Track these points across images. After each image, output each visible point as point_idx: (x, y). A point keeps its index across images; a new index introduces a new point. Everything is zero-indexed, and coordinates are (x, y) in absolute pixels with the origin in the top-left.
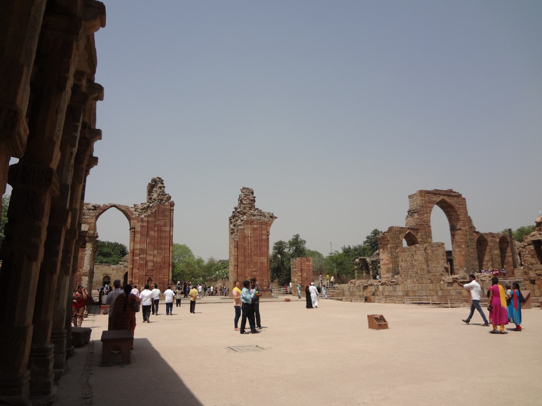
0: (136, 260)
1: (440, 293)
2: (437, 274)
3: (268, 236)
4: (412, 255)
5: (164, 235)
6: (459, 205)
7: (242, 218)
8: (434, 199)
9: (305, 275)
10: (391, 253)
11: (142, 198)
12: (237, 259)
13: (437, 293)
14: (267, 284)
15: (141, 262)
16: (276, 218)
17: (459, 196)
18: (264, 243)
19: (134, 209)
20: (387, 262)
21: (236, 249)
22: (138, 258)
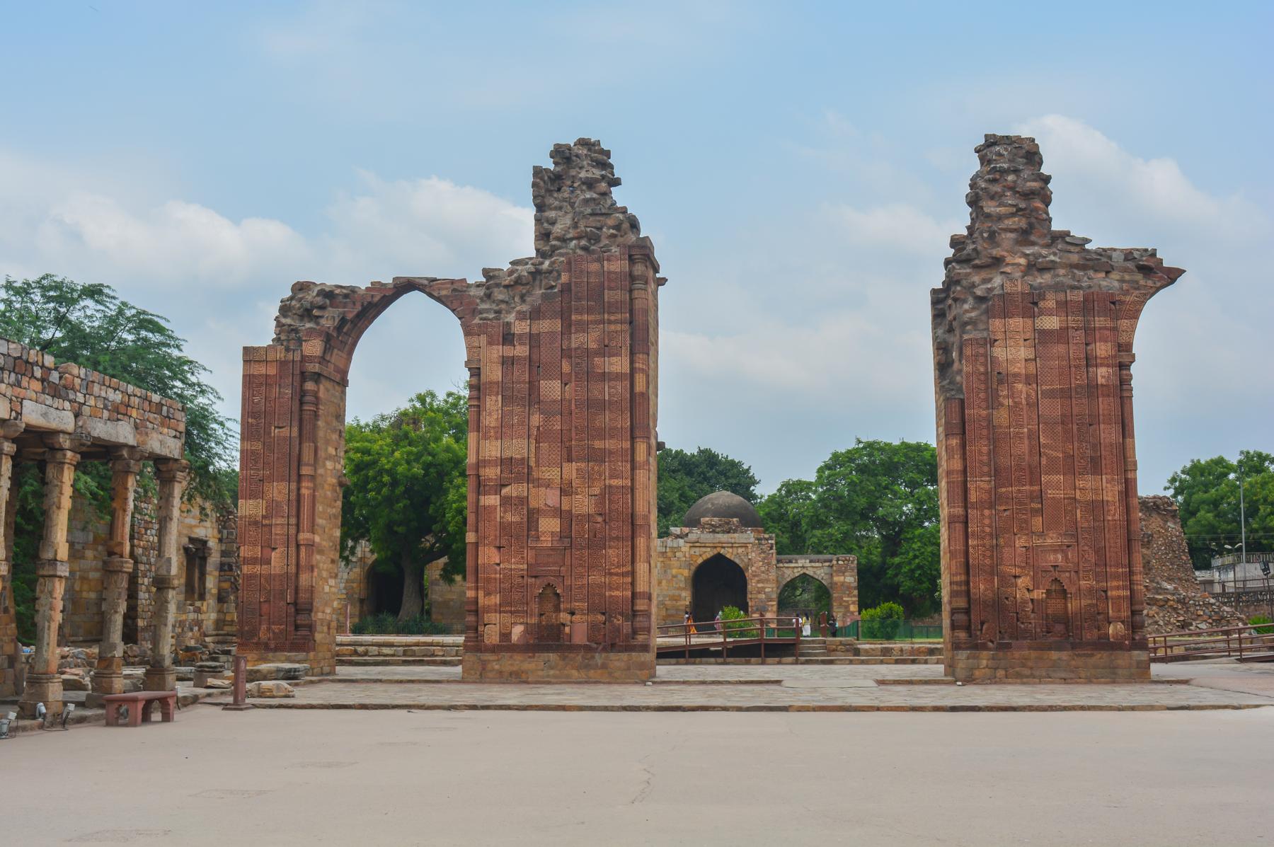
0: (490, 509)
3: (1124, 367)
5: (607, 391)
7: (979, 292)
11: (513, 235)
14: (1125, 613)
15: (511, 518)
16: (1173, 275)
19: (481, 292)
21: (954, 442)
22: (491, 500)
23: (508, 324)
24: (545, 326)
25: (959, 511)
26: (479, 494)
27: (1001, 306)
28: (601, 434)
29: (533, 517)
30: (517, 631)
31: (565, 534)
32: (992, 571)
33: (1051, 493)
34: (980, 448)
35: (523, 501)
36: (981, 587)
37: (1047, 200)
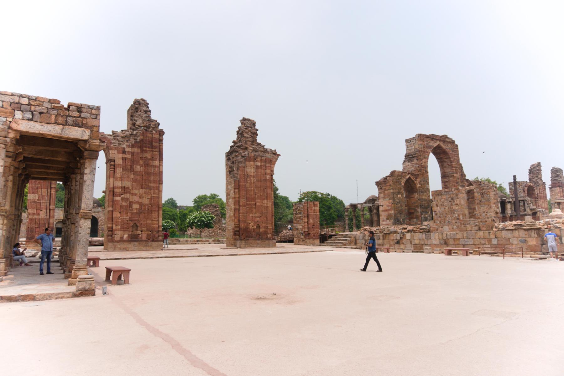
0: (118, 201)
1: (495, 242)
2: (487, 219)
3: (272, 176)
4: (452, 199)
5: (153, 170)
6: (453, 151)
7: (243, 154)
8: (431, 144)
9: (311, 221)
10: (393, 199)
12: (237, 202)
13: (490, 241)
15: (123, 204)
16: (279, 155)
17: (453, 142)
18: (269, 184)
20: (387, 208)
21: (237, 190)
22: (118, 198)
23: (124, 148)
24: (135, 150)
25: (238, 207)
26: (113, 196)
27: (247, 159)
28: (151, 182)
29: (131, 204)
30: (125, 236)
31: (140, 209)
32: (245, 222)
33: (257, 204)
34: (243, 192)
35: (128, 199)
36: (242, 225)
37: (257, 135)
